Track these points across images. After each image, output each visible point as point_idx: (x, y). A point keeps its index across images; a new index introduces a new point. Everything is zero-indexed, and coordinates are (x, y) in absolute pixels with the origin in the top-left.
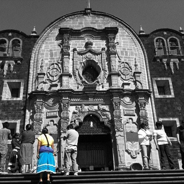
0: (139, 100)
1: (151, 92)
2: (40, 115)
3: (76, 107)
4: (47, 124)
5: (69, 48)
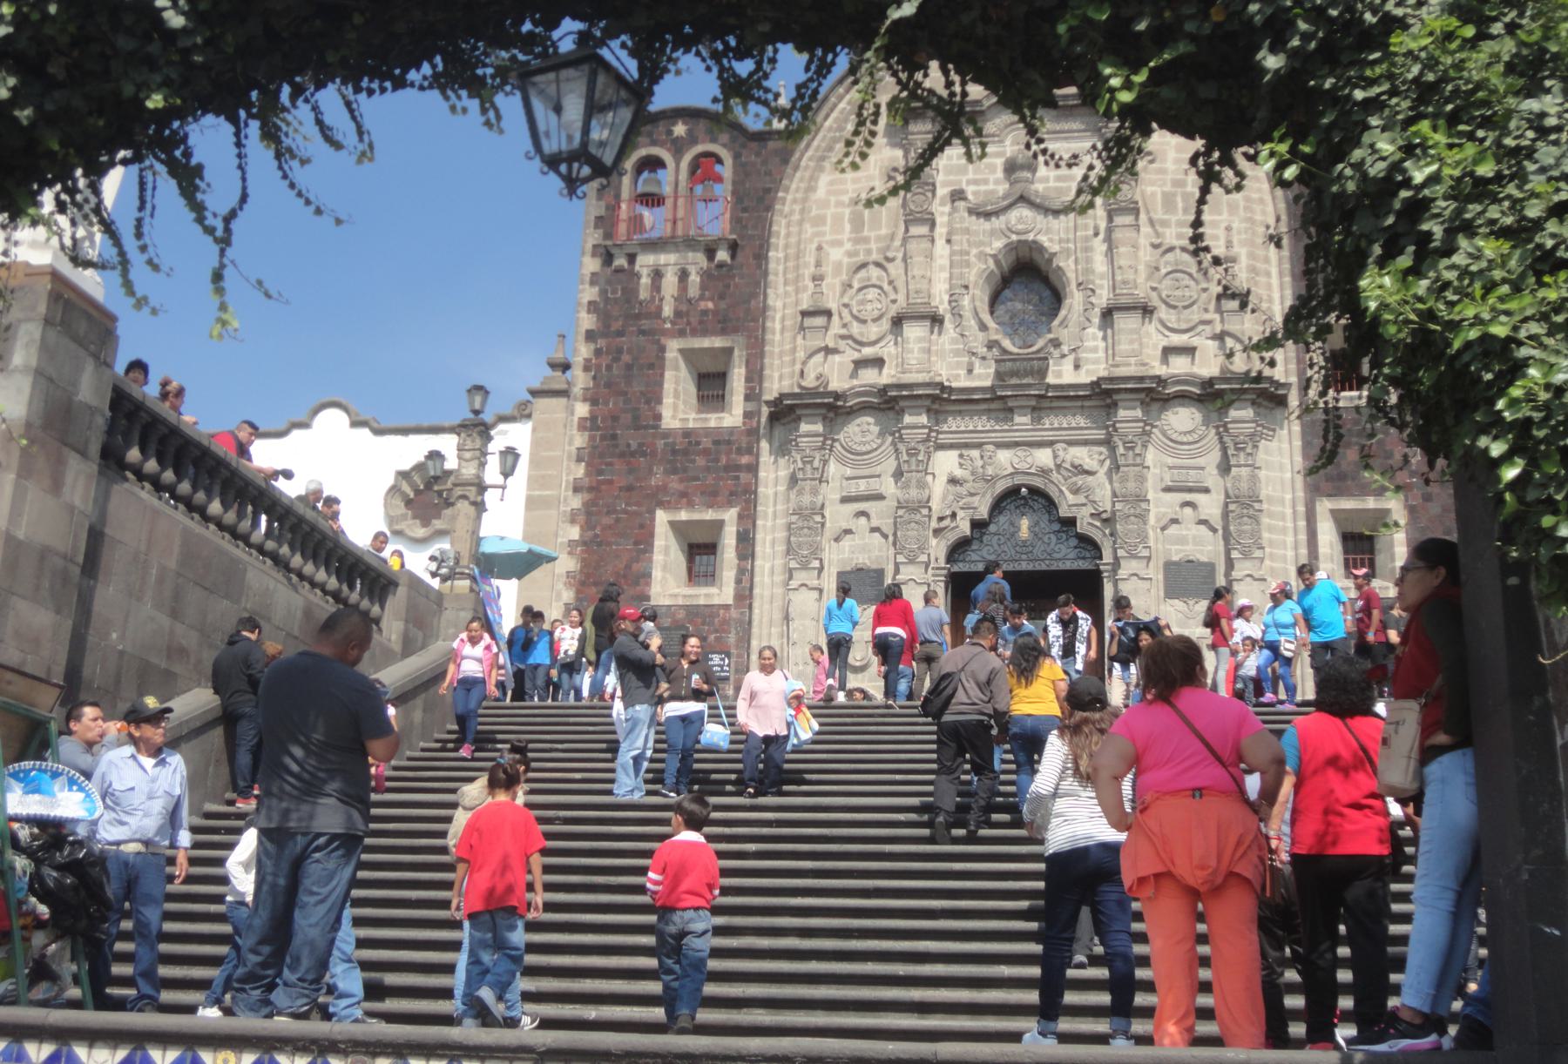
0: (1231, 422)
1: (1287, 386)
2: (815, 492)
3: (961, 456)
4: (845, 526)
5: (934, 192)
